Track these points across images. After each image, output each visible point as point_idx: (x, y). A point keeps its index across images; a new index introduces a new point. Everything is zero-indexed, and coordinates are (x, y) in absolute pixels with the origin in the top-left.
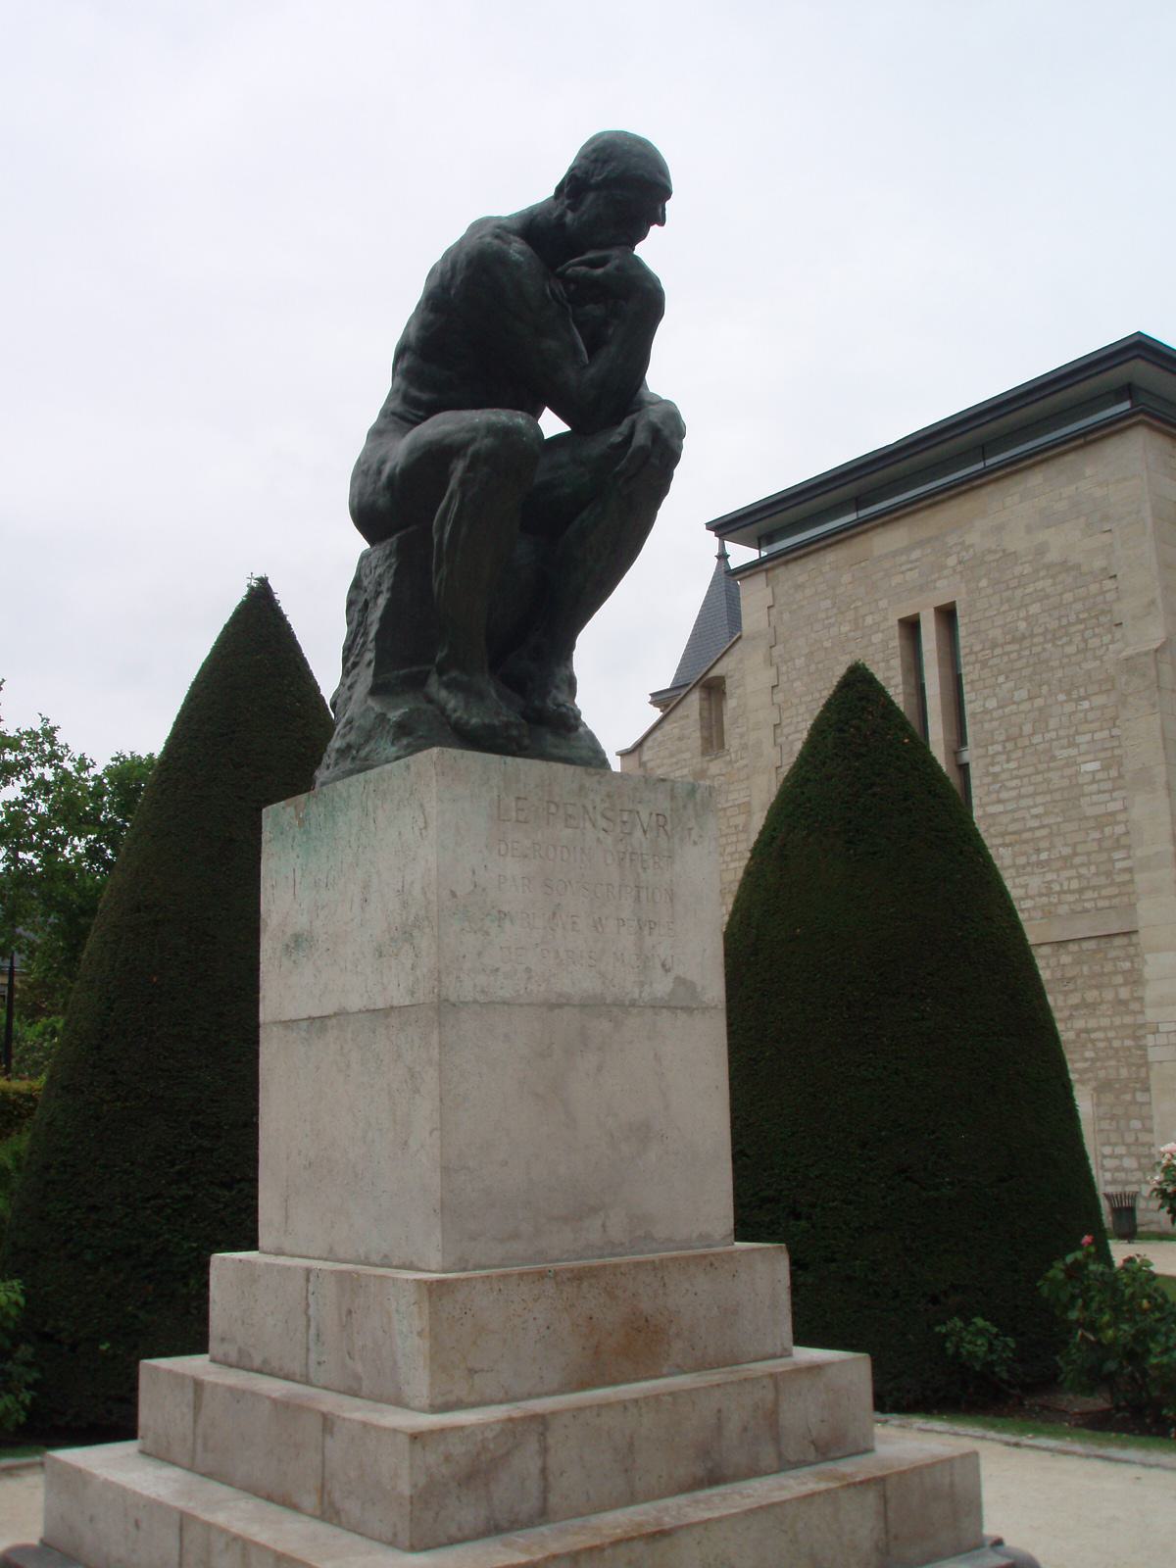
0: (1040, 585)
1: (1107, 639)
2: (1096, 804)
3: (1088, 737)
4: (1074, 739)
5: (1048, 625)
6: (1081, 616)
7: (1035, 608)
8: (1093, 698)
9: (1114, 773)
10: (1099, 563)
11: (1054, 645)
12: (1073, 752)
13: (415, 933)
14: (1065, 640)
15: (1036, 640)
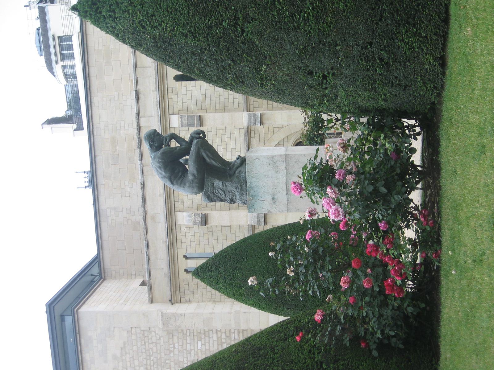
0: (128, 359)
1: (153, 334)
2: (213, 344)
3: (188, 345)
4: (188, 351)
5: (144, 358)
6: (143, 343)
7: (136, 363)
8: (174, 342)
9: (203, 336)
10: (125, 334)
11: (152, 356)
12: (193, 352)
13: (274, 161)
14: (151, 351)
15: (148, 363)
